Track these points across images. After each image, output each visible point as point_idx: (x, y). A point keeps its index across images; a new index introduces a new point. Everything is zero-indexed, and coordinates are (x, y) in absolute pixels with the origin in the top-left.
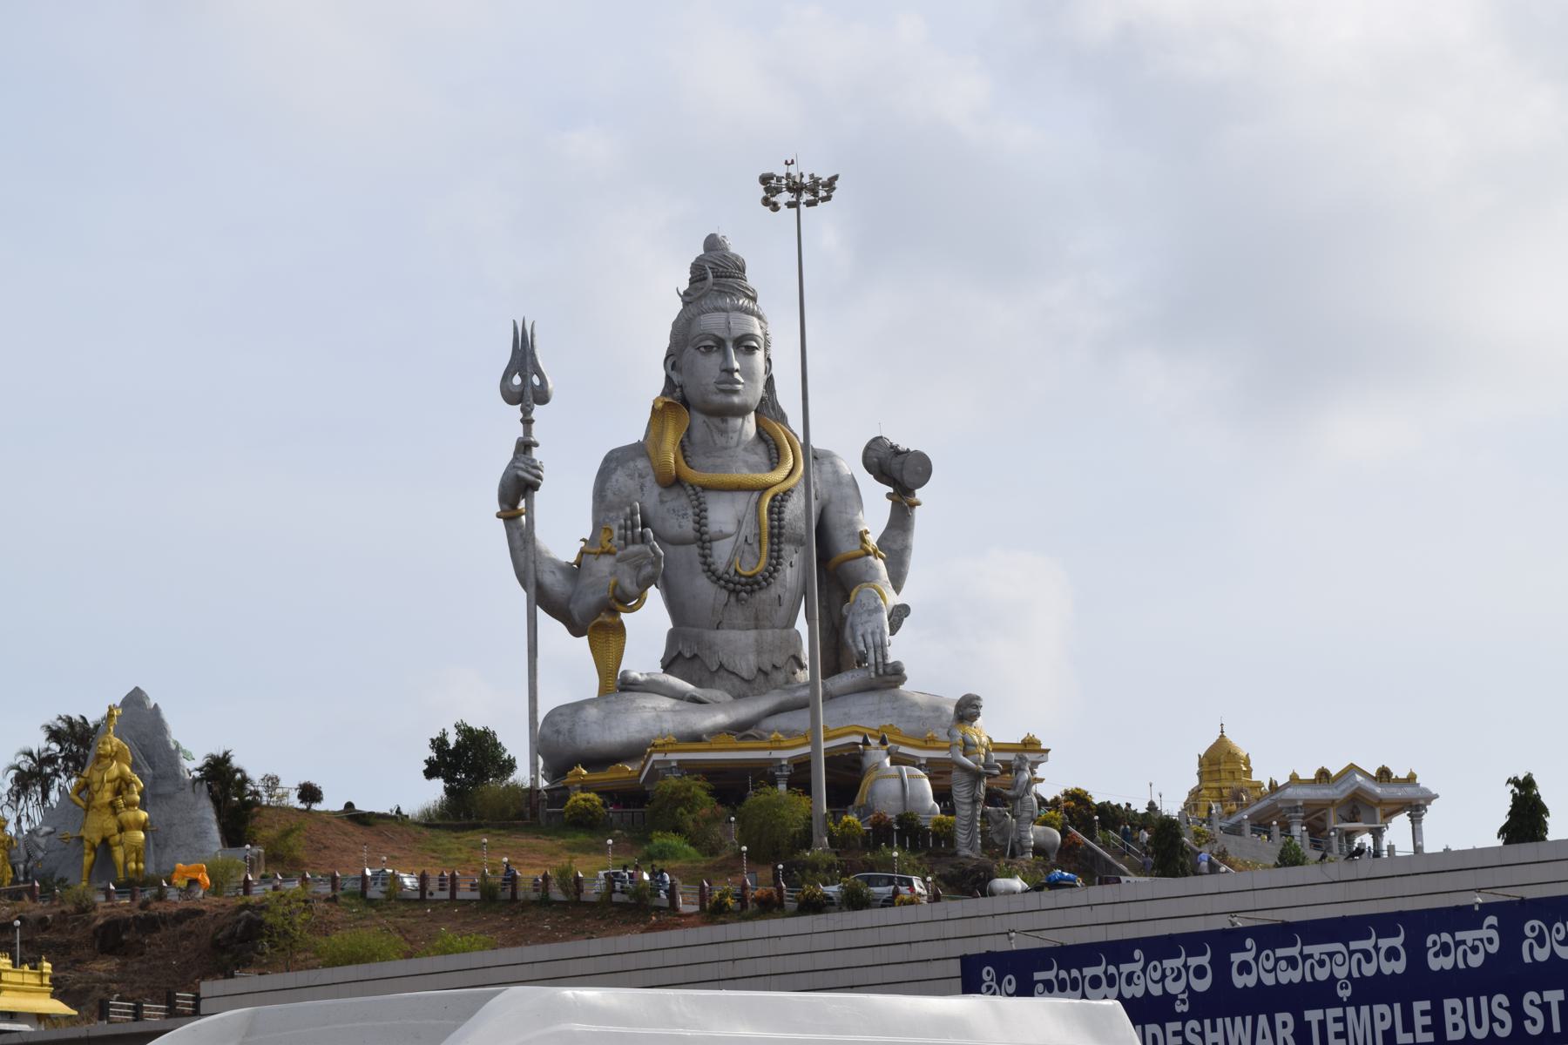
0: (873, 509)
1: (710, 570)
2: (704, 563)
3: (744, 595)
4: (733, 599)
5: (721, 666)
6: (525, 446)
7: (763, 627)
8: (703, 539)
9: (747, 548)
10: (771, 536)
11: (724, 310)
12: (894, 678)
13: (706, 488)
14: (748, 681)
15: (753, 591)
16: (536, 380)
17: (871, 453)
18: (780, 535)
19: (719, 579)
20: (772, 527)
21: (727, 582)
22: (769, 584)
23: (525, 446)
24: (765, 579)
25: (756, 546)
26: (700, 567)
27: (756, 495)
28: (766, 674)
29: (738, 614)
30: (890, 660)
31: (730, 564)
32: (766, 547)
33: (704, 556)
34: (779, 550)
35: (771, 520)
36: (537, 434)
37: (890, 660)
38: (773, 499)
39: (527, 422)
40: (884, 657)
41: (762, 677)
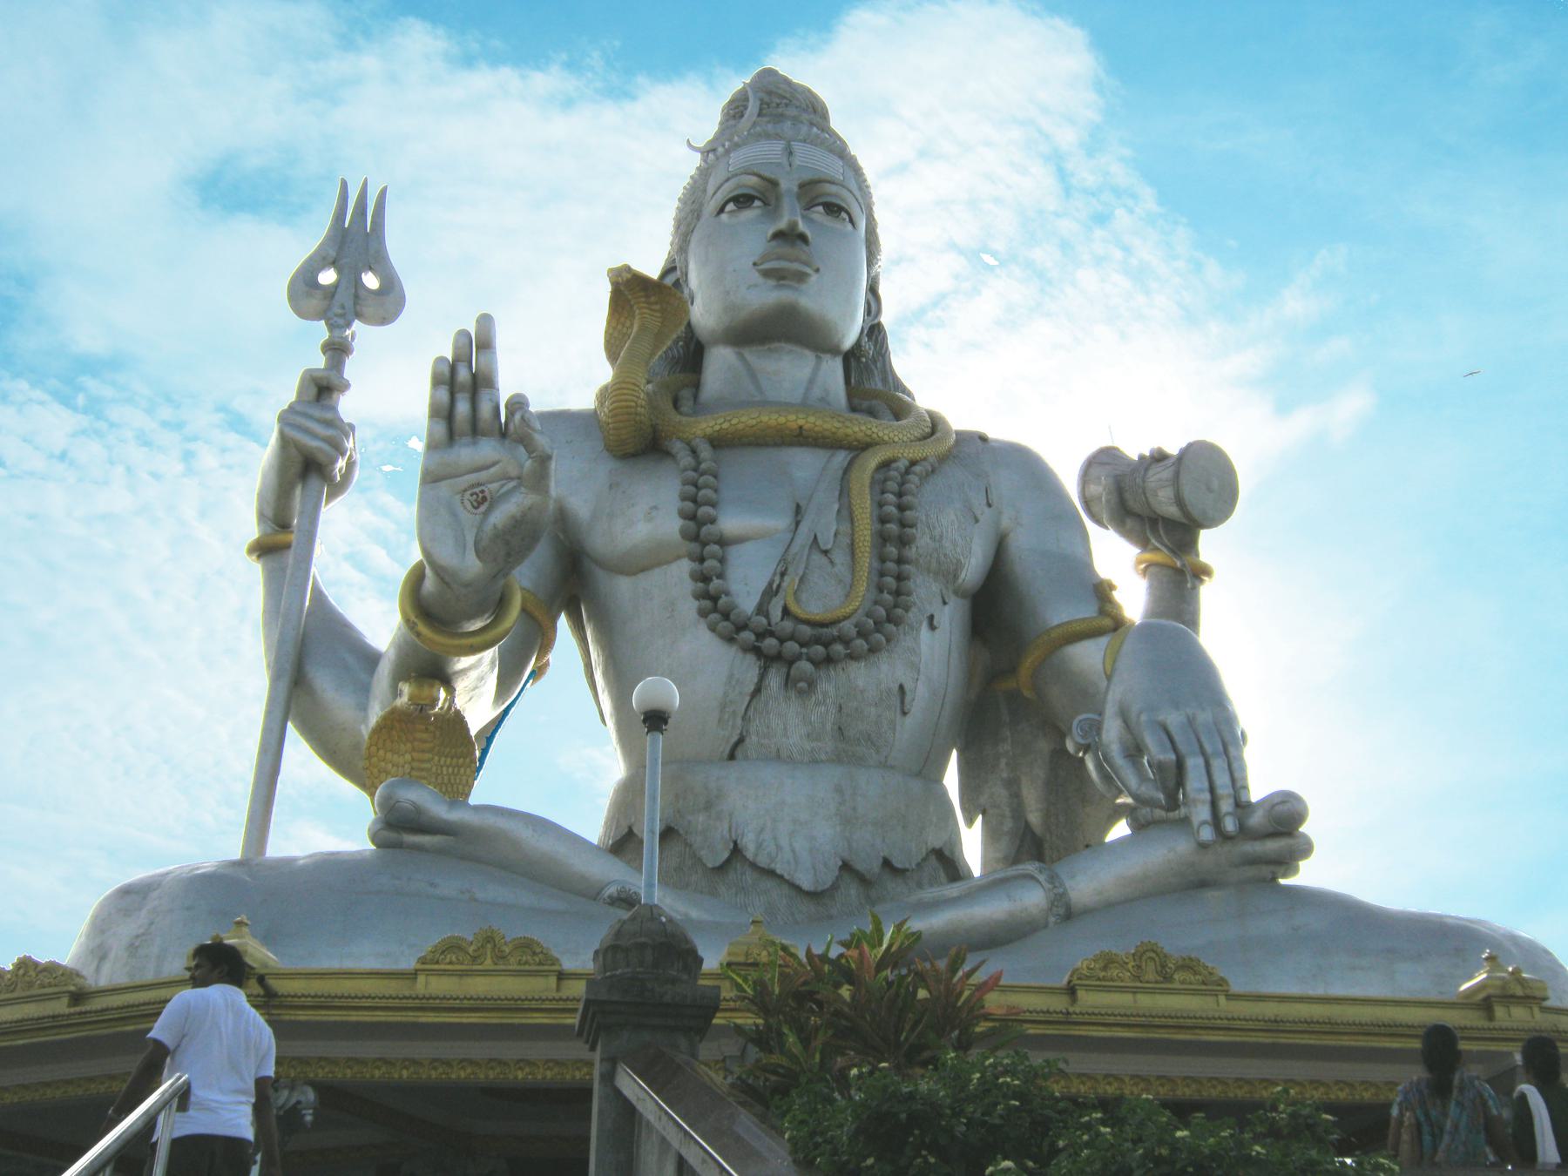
0: (1117, 560)
1: (713, 603)
2: (703, 595)
3: (805, 666)
4: (774, 680)
5: (736, 851)
6: (322, 389)
7: (859, 761)
8: (704, 543)
9: (817, 558)
10: (883, 538)
11: (778, 137)
12: (1272, 846)
13: (719, 442)
14: (814, 895)
15: (829, 660)
16: (371, 281)
17: (1095, 471)
18: (903, 542)
19: (742, 627)
20: (883, 520)
21: (760, 636)
22: (873, 650)
23: (322, 389)
24: (862, 634)
25: (840, 557)
26: (689, 607)
27: (841, 457)
28: (863, 880)
29: (788, 721)
30: (1258, 789)
31: (770, 592)
32: (866, 560)
33: (705, 578)
34: (900, 578)
35: (881, 505)
36: (352, 368)
37: (1258, 789)
38: (886, 465)
39: (337, 350)
40: (1238, 784)
41: (852, 891)
